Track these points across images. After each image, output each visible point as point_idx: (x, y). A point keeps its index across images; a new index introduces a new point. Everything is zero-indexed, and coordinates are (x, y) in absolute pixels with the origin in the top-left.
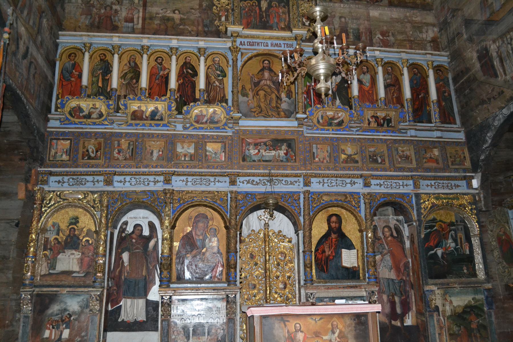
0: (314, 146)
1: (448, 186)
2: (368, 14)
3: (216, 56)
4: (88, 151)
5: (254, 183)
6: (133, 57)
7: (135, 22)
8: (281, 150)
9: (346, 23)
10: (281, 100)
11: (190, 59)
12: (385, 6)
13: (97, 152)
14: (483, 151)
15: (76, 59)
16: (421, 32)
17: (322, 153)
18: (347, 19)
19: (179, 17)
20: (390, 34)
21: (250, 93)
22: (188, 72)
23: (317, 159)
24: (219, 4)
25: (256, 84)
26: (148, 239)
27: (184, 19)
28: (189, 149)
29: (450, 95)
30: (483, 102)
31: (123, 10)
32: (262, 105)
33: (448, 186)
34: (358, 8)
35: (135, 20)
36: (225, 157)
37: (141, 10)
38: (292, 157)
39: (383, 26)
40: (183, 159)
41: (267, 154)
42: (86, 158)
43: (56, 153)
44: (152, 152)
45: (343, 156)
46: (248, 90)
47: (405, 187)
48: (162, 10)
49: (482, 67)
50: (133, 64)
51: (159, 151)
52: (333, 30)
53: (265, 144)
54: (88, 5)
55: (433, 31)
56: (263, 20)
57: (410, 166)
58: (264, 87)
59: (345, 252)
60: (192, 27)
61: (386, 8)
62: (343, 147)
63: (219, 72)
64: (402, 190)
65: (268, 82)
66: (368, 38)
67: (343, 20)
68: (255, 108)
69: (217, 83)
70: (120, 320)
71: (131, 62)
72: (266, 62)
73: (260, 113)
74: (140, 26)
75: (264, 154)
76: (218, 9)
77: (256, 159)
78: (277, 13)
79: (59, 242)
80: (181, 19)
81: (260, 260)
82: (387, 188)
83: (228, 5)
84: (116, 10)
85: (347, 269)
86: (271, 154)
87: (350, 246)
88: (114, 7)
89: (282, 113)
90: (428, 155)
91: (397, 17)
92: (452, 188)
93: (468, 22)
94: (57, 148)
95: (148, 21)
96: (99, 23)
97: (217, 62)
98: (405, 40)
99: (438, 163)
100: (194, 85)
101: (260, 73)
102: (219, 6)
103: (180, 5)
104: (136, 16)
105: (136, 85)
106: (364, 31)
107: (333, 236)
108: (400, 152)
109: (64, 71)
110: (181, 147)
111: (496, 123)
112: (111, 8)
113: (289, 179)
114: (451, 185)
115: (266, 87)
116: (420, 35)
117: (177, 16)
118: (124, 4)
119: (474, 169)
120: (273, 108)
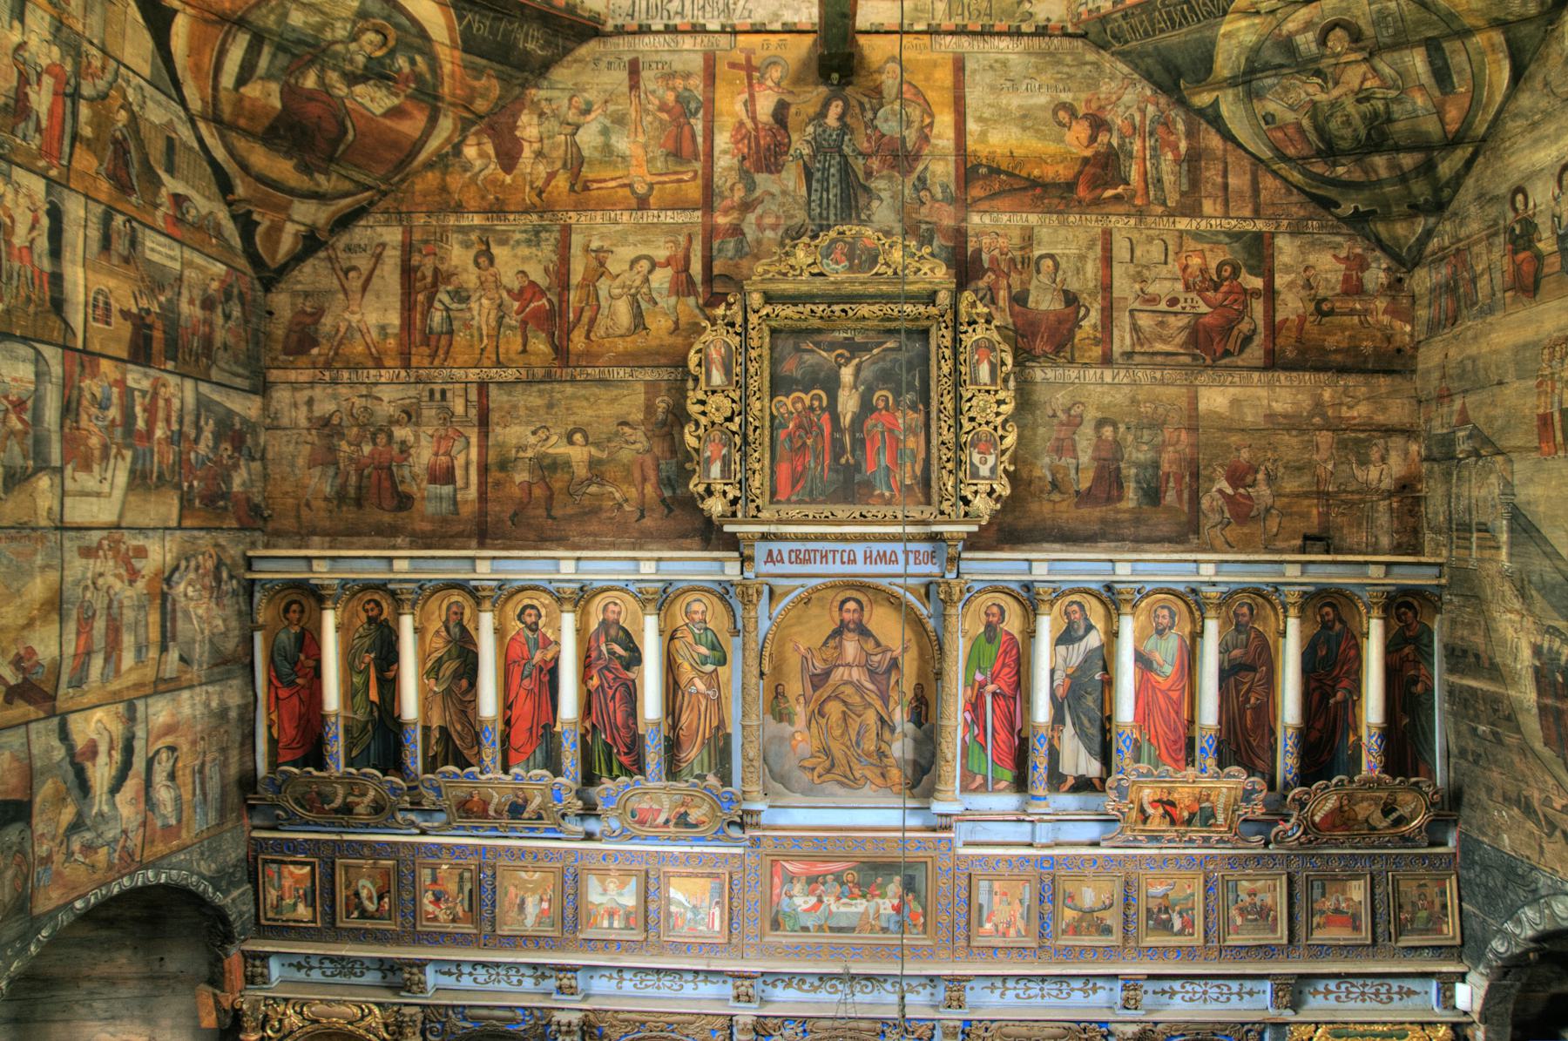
0: (984, 885)
1: (1377, 993)
2: (1194, 401)
3: (697, 595)
4: (357, 894)
5: (806, 987)
6: (454, 609)
7: (460, 483)
8: (883, 895)
9: (1117, 445)
10: (893, 730)
11: (616, 609)
12: (1256, 369)
13: (381, 898)
15: (305, 619)
16: (1364, 462)
17: (1004, 910)
18: (1122, 428)
19: (586, 457)
20: (1260, 476)
22: (612, 658)
23: (988, 926)
24: (704, 413)
25: (819, 680)
27: (600, 462)
28: (621, 895)
29: (1429, 690)
30: (1528, 810)
31: (423, 443)
32: (837, 749)
33: (1377, 993)
34: (1163, 383)
35: (459, 473)
36: (722, 922)
37: (474, 440)
38: (915, 916)
39: (1237, 450)
40: (606, 924)
41: (843, 909)
42: (356, 914)
43: (281, 898)
44: (523, 902)
45: (1069, 914)
46: (792, 701)
47: (1246, 997)
48: (534, 433)
49: (1543, 710)
50: (456, 631)
51: (542, 900)
52: (1073, 472)
54: (326, 431)
55: (1406, 453)
56: (843, 461)
57: (1266, 938)
58: (842, 688)
60: (625, 488)
61: (1256, 375)
62: (1070, 887)
63: (704, 650)
65: (856, 674)
66: (1186, 496)
67: (1108, 432)
68: (812, 756)
69: (700, 685)
71: (452, 625)
72: (851, 605)
73: (828, 771)
74: (473, 493)
75: (833, 908)
76: (701, 431)
77: (809, 924)
78: (891, 431)
80: (593, 464)
82: (1191, 1000)
83: (730, 419)
84: (403, 442)
86: (853, 909)
88: (400, 433)
89: (894, 773)
90: (1329, 904)
91: (1289, 408)
92: (1391, 999)
93: (1524, 527)
94: (281, 887)
95: (495, 475)
96: (359, 488)
97: (697, 617)
98: (1306, 495)
99: (1357, 928)
101: (832, 643)
102: (703, 421)
103: (590, 412)
104: (460, 461)
105: (468, 698)
106: (1174, 468)
108: (1243, 896)
109: (277, 659)
110: (600, 890)
112: (390, 436)
114: (1389, 991)
115: (848, 690)
116: (1360, 474)
117: (578, 454)
118: (425, 420)
120: (869, 755)
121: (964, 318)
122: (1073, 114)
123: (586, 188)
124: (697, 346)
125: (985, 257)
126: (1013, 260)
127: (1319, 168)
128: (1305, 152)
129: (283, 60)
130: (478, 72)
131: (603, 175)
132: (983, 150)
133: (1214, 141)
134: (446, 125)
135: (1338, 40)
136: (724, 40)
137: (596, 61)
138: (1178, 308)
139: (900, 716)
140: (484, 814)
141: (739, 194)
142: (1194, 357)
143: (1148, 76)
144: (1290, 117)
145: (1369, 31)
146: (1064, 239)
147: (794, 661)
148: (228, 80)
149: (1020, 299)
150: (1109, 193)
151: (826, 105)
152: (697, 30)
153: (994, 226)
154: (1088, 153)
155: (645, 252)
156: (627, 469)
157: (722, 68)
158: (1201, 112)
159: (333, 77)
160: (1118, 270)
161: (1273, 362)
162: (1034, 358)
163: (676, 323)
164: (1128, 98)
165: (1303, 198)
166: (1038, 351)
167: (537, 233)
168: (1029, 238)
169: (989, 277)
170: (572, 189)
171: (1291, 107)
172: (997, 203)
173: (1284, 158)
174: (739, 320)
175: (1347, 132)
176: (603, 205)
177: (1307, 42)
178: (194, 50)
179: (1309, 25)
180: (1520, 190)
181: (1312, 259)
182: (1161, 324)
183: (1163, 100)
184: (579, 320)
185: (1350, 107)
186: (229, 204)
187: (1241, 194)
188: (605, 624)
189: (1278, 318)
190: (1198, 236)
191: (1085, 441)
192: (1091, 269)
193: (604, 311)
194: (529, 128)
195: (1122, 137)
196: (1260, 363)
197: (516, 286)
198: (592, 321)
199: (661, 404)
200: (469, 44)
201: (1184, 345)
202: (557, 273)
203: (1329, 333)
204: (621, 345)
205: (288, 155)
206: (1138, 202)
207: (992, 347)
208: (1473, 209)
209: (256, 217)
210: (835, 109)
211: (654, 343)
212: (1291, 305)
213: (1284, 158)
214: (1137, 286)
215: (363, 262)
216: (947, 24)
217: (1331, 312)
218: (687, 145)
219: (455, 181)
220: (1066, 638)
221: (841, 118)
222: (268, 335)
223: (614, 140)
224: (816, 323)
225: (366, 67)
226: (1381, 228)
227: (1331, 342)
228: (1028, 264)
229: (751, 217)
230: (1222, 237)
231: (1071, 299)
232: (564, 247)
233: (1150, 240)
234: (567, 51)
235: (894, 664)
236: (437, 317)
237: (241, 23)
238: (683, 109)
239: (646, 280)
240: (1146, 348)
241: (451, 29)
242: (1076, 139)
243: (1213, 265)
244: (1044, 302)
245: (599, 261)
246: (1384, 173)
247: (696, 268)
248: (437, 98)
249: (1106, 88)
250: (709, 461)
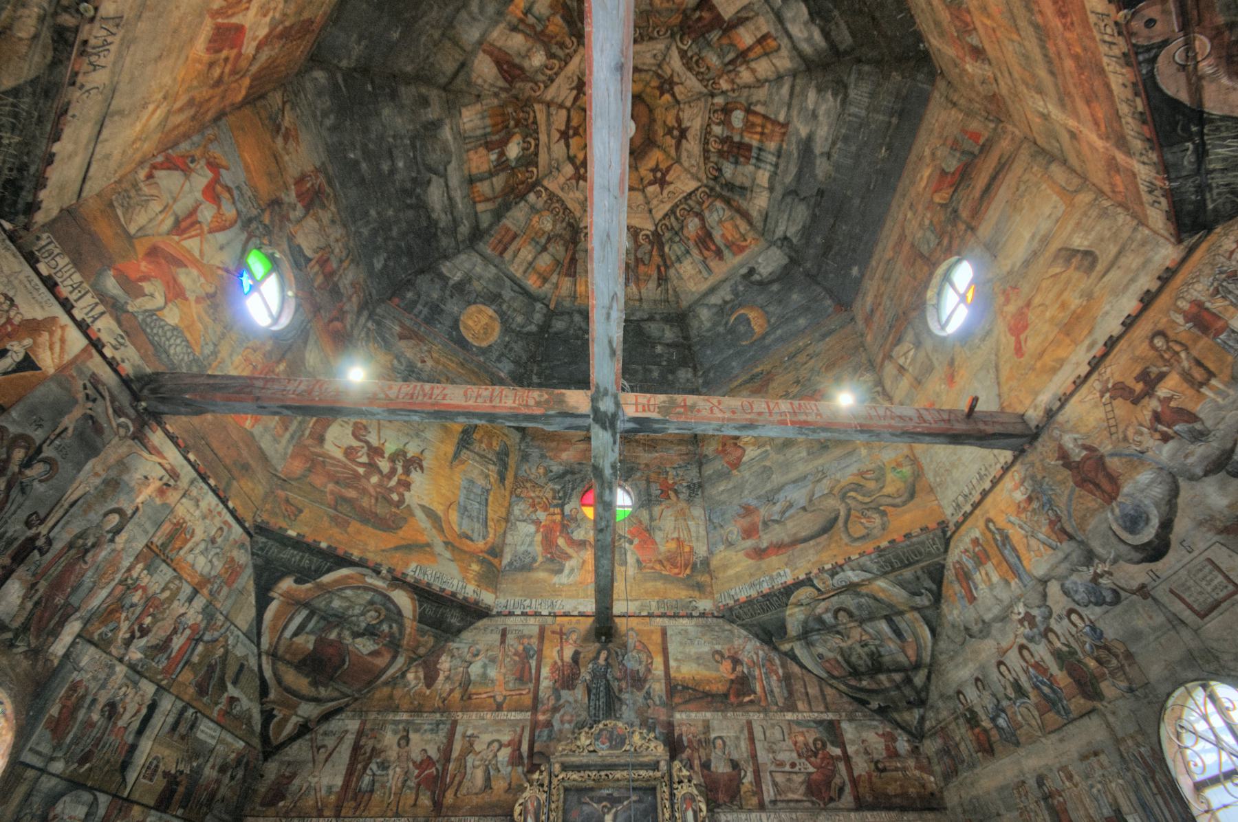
121: (676, 780)
122: (722, 656)
123: (470, 698)
124: (521, 801)
125: (684, 739)
126: (700, 741)
127: (853, 682)
128: (843, 674)
129: (322, 624)
130: (423, 633)
131: (480, 691)
132: (679, 677)
133: (796, 669)
134: (400, 661)
135: (843, 617)
136: (550, 620)
137: (485, 629)
138: (796, 769)
141: (552, 702)
142: (813, 802)
143: (757, 636)
144: (831, 655)
145: (856, 612)
146: (725, 727)
148: (288, 634)
149: (706, 766)
150: (747, 699)
151: (599, 653)
152: (537, 614)
153: (688, 720)
154: (733, 677)
155: (496, 736)
157: (548, 633)
158: (786, 654)
159: (347, 633)
160: (759, 746)
162: (719, 806)
163: (510, 784)
164: (750, 648)
165: (849, 700)
166: (721, 801)
167: (438, 725)
168: (707, 727)
169: (688, 752)
170: (462, 698)
171: (830, 650)
172: (689, 706)
173: (834, 677)
174: (546, 783)
175: (861, 662)
176: (478, 708)
177: (828, 618)
178: (276, 617)
179: (827, 610)
180: (959, 692)
181: (864, 735)
182: (789, 780)
183: (766, 648)
184: (452, 782)
185: (859, 650)
186: (262, 704)
187: (816, 697)
189: (856, 774)
190: (798, 723)
192: (744, 745)
193: (468, 776)
194: (445, 663)
195: (749, 668)
196: (852, 805)
197: (419, 759)
198: (460, 783)
200: (422, 619)
201: (805, 794)
202: (445, 750)
203: (887, 783)
204: (475, 800)
205: (307, 676)
206: (763, 704)
207: (693, 799)
208: (940, 704)
209: (275, 712)
210: (603, 655)
211: (495, 799)
212: (861, 767)
213: (834, 677)
214: (771, 756)
215: (330, 742)
216: (657, 612)
217: (884, 770)
218: (526, 673)
219: (398, 693)
221: (606, 660)
222: (255, 791)
223: (489, 671)
224: (591, 783)
225: (365, 629)
226: (896, 716)
227: (891, 790)
228: (708, 743)
229: (558, 716)
230: (812, 724)
231: (735, 765)
233: (773, 726)
234: (472, 624)
236: (367, 779)
237: (306, 605)
238: (526, 655)
239: (496, 756)
240: (783, 797)
241: (414, 611)
242: (725, 670)
243: (811, 741)
244: (721, 768)
245: (470, 741)
246: (887, 684)
247: (525, 747)
248: (399, 646)
249: (737, 642)
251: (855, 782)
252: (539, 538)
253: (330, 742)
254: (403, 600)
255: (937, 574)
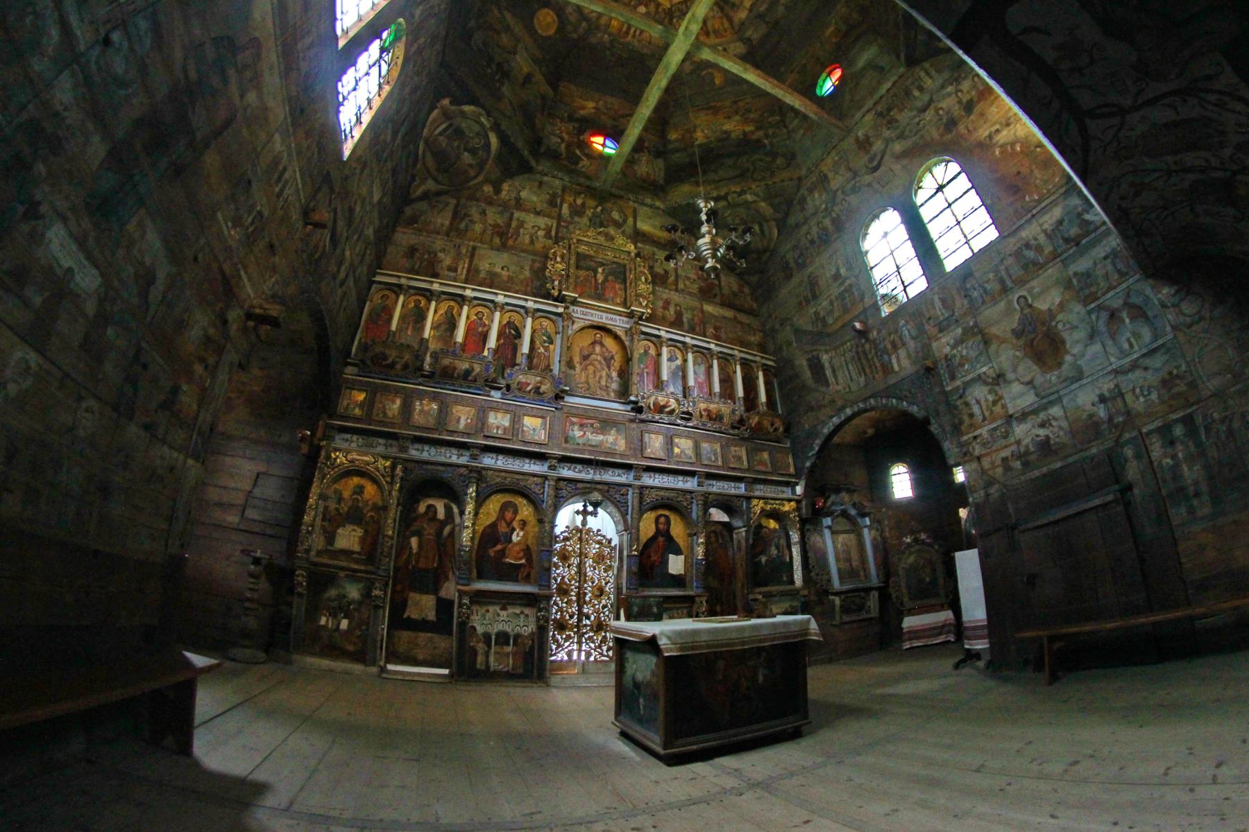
14: (808, 458)
21: (578, 365)
22: (511, 334)
26: (443, 524)
30: (812, 409)
53: (592, 425)
59: (672, 557)
64: (733, 491)
69: (542, 350)
70: (405, 616)
74: (463, 277)
77: (580, 441)
79: (340, 514)
81: (575, 561)
85: (673, 576)
87: (678, 552)
100: (515, 349)
107: (661, 539)
111: (826, 431)
113: (617, 471)
119: (797, 475)
134: (480, 178)
139: (614, 374)
140: (452, 377)
147: (576, 350)
148: (437, 132)
156: (522, 282)
161: (723, 305)
176: (527, 211)
188: (508, 323)
191: (672, 309)
194: (505, 186)
199: (537, 265)
200: (500, 158)
210: (599, 209)
212: (726, 291)
220: (670, 360)
231: (666, 272)
232: (511, 219)
235: (612, 357)
236: (462, 226)
245: (521, 224)
247: (553, 233)
250: (553, 281)
251: (722, 295)
252: (563, 146)
253: (441, 206)
254: (493, 139)
255: (789, 203)
